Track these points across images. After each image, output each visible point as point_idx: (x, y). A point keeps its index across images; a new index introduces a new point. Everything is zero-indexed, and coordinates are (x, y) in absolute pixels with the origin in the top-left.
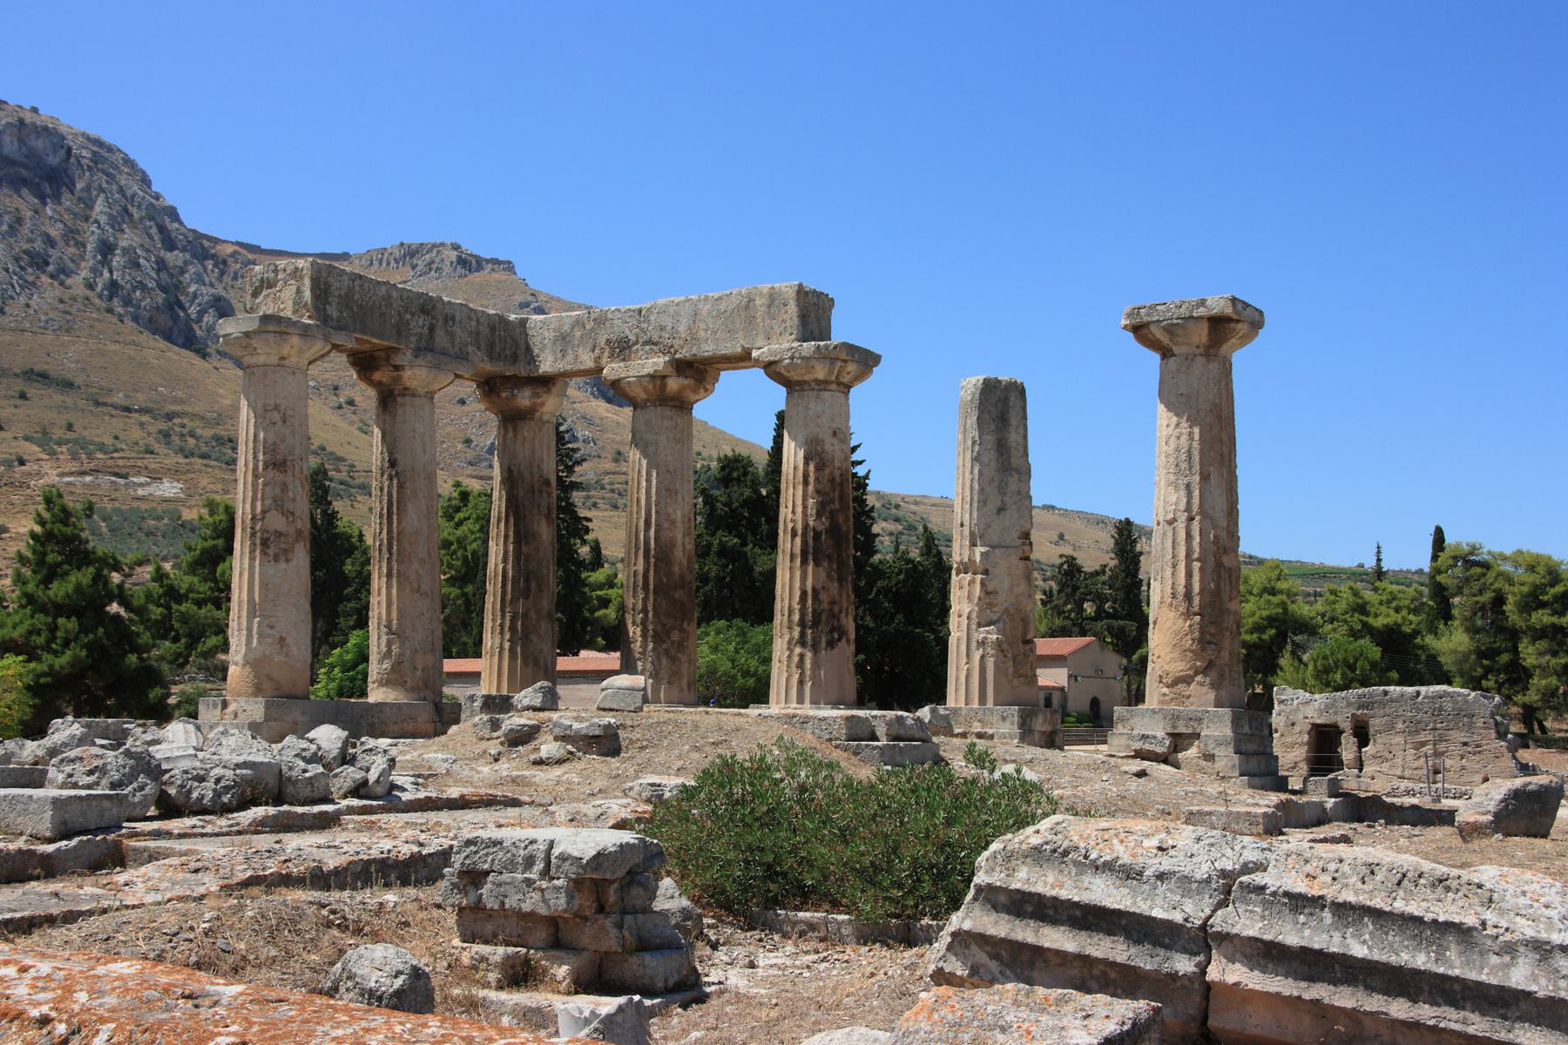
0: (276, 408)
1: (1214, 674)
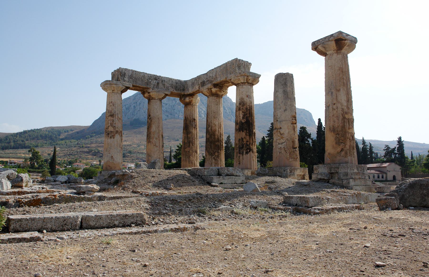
0: (112, 102)
1: (343, 153)
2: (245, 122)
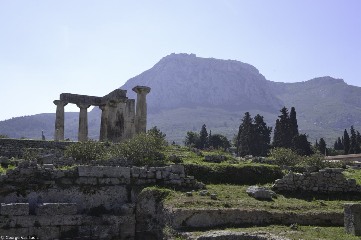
0: (58, 111)
2: (119, 121)
